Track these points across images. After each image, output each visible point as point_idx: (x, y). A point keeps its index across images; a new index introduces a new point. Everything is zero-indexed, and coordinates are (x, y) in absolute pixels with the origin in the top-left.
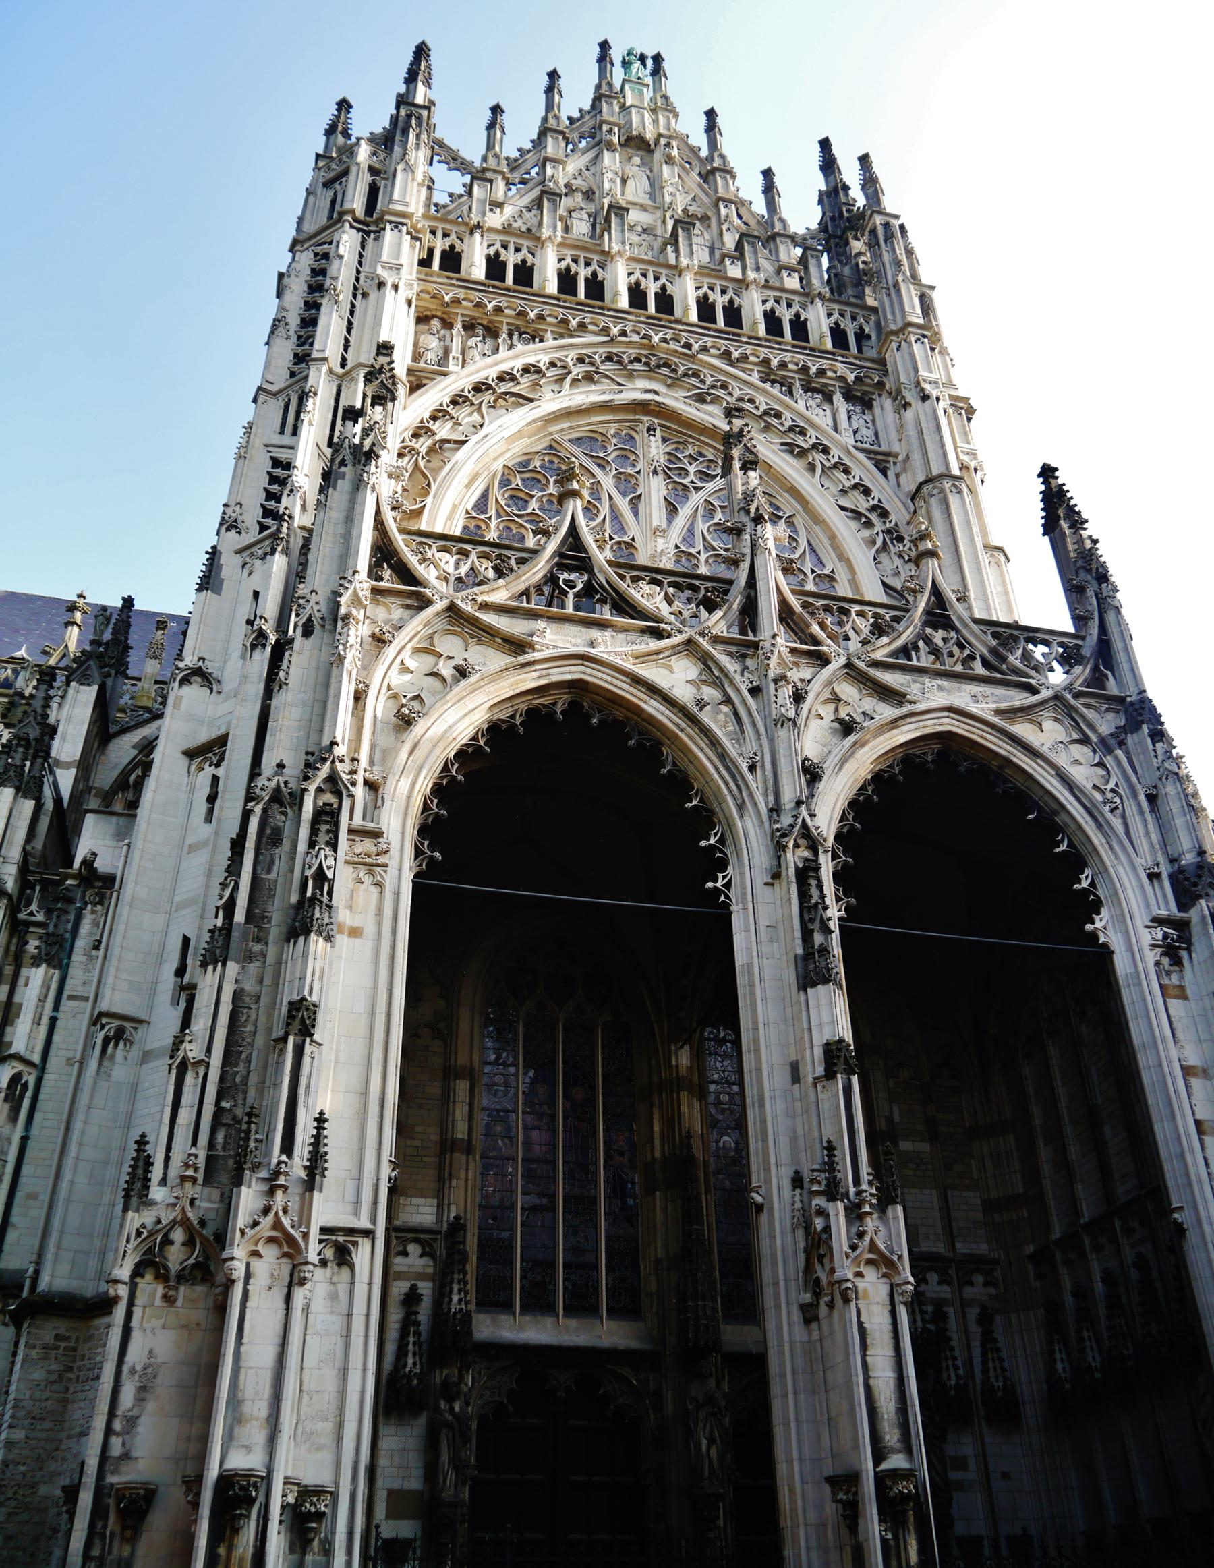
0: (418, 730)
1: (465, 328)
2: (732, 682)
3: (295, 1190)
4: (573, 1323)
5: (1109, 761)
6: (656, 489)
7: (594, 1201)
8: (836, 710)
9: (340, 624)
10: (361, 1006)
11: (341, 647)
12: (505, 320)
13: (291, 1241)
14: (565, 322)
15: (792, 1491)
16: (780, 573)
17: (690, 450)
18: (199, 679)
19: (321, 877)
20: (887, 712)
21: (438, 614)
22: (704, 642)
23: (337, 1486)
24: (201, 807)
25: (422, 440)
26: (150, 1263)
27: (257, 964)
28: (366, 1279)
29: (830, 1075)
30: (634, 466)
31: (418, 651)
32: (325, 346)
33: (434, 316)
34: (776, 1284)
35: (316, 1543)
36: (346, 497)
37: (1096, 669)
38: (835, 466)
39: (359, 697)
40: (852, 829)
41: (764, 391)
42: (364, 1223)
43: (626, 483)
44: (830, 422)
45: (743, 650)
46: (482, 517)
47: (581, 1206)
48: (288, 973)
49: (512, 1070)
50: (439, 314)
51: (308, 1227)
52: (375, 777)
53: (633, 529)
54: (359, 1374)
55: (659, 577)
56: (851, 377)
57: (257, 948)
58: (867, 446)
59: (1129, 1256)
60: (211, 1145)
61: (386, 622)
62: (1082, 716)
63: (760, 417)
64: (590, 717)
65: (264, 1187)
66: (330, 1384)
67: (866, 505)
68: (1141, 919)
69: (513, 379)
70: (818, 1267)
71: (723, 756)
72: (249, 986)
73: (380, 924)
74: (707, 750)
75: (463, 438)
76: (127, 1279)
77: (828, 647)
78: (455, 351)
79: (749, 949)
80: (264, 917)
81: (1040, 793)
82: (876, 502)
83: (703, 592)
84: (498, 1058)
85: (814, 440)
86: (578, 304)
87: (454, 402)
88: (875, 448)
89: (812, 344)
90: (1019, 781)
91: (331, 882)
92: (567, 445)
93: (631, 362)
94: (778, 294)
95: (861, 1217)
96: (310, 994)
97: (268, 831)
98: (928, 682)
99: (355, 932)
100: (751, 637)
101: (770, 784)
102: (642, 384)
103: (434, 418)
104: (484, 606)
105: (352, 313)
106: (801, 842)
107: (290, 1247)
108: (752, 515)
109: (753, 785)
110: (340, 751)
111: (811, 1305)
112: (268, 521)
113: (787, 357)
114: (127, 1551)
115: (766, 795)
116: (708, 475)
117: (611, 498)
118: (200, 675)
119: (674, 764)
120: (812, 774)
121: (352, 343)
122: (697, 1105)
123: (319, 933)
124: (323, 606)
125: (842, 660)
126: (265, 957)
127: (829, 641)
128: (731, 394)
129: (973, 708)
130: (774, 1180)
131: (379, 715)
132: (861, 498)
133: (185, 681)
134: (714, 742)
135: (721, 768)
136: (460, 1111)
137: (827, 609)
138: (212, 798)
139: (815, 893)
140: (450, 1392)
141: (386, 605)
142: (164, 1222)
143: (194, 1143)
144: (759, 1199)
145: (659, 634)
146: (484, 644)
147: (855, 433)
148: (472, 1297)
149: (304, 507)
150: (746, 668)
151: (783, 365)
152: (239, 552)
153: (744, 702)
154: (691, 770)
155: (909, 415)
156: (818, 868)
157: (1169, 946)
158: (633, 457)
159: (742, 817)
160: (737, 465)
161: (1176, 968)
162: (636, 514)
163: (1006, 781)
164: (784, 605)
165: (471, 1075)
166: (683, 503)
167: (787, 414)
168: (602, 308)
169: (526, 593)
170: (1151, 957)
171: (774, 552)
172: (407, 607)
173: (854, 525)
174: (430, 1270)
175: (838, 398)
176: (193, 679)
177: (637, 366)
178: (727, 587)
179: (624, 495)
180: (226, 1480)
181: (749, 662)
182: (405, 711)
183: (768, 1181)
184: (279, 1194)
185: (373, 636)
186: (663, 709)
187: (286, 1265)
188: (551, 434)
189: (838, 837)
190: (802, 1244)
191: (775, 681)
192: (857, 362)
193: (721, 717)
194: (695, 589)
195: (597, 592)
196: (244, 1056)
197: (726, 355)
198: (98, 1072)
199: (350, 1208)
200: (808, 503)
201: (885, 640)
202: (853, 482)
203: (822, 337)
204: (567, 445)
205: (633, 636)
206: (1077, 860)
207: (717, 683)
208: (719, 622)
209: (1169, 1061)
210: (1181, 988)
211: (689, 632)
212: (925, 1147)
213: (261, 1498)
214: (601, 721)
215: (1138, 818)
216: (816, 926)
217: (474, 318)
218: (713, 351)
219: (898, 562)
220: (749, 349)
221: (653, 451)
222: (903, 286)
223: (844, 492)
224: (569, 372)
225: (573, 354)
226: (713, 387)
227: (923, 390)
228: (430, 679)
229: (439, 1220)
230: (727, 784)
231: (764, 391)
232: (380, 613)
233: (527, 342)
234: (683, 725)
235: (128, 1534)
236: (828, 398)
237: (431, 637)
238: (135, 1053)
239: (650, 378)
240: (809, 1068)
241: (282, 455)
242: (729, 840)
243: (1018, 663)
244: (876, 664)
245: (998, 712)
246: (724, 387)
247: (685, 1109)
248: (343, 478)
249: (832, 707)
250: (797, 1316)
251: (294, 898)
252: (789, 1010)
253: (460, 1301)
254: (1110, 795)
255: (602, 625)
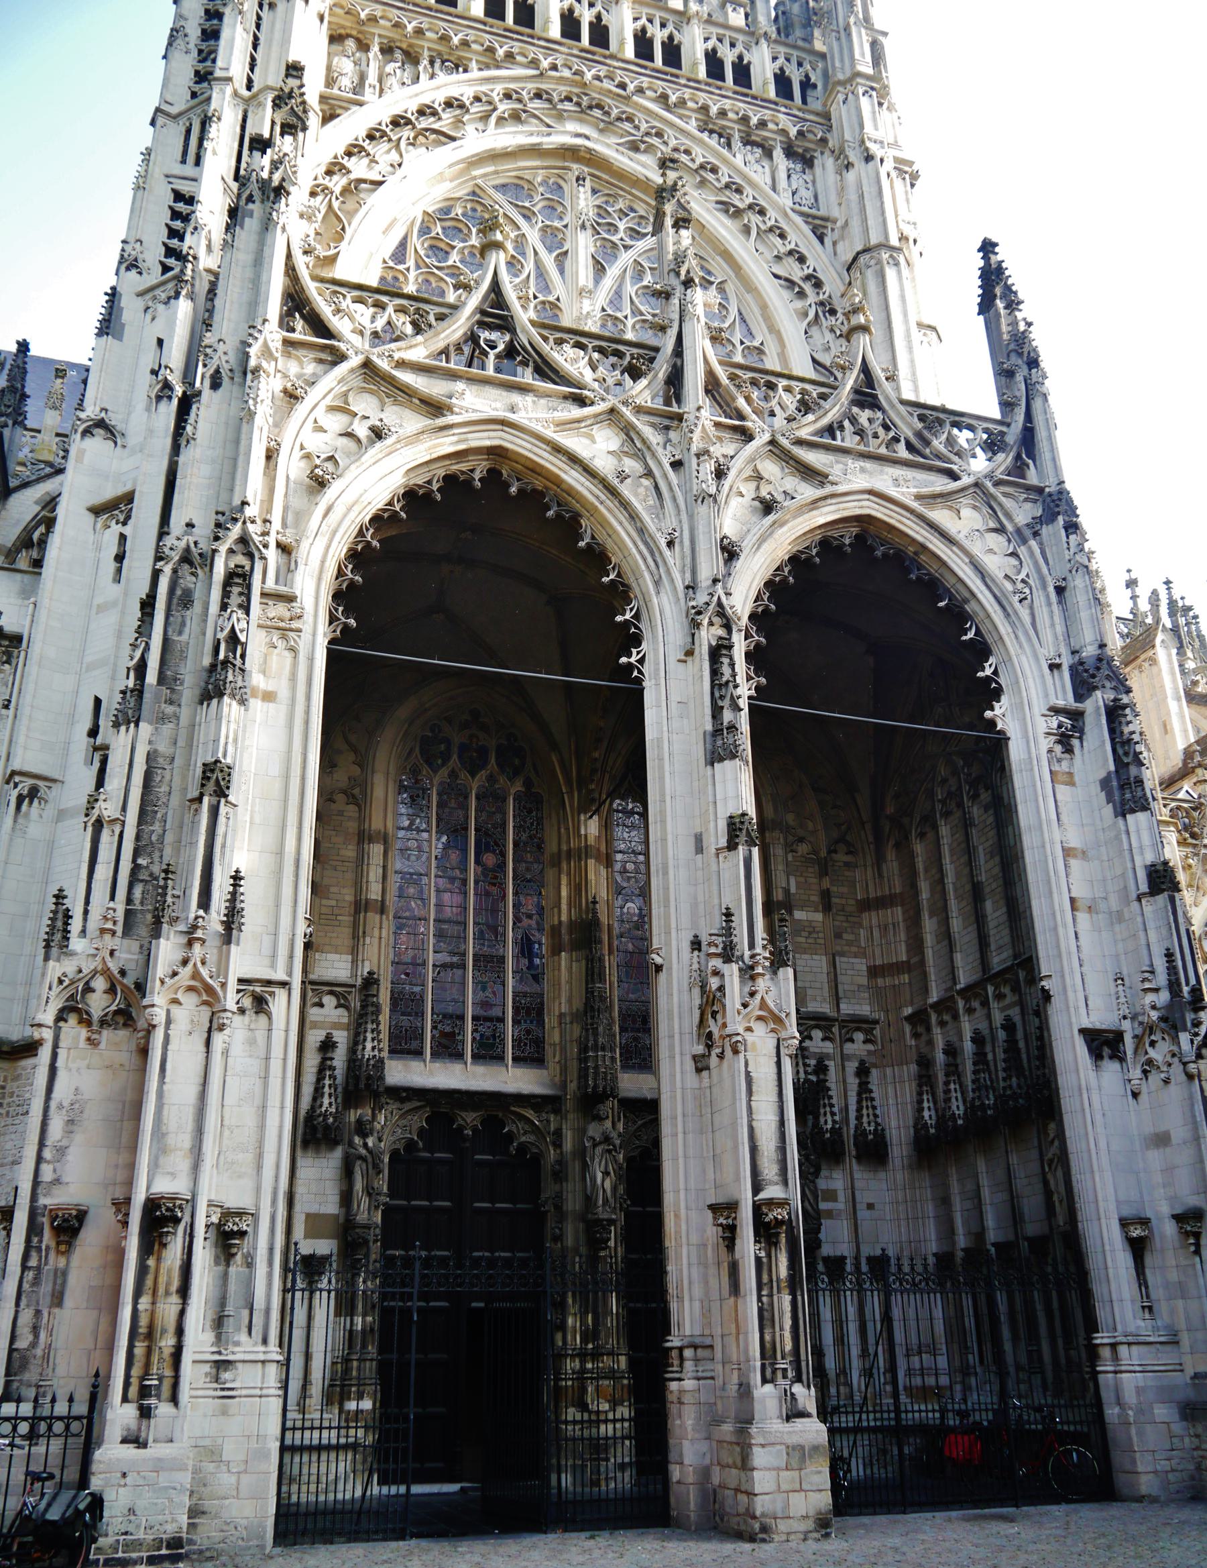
0: (331, 493)
1: (382, 51)
2: (654, 455)
3: (213, 943)
4: (480, 1069)
5: (1022, 551)
6: (584, 246)
7: (502, 960)
8: (758, 488)
9: (249, 376)
10: (275, 769)
11: (251, 402)
12: (426, 44)
13: (209, 990)
14: (491, 50)
15: (677, 1216)
16: (707, 343)
17: (621, 204)
18: (101, 432)
19: (233, 639)
20: (808, 492)
21: (352, 371)
22: (627, 412)
23: (258, 1208)
24: (112, 566)
25: (336, 178)
26: (72, 1009)
27: (171, 725)
28: (283, 1026)
29: (732, 846)
30: (561, 218)
31: (332, 409)
32: (229, 63)
33: (349, 36)
34: (671, 1037)
35: (239, 1257)
36: (254, 238)
37: (1018, 457)
38: (771, 230)
39: (270, 455)
40: (766, 610)
41: (701, 142)
42: (280, 975)
43: (552, 238)
44: (769, 181)
45: (666, 422)
46: (401, 267)
47: (490, 964)
48: (202, 735)
49: (425, 835)
50: (354, 33)
51: (226, 977)
52: (287, 540)
53: (559, 289)
54: (277, 1111)
55: (584, 340)
56: (793, 132)
57: (169, 709)
58: (806, 209)
59: (998, 1018)
60: (129, 901)
61: (299, 376)
62: (1000, 505)
63: (696, 171)
64: (508, 486)
65: (183, 940)
66: (249, 1119)
67: (801, 274)
68: (1039, 707)
69: (434, 113)
70: (711, 1022)
71: (642, 531)
72: (163, 747)
73: (293, 689)
74: (626, 524)
75: (380, 178)
76: (51, 1023)
77: (753, 423)
78: (372, 78)
79: (659, 723)
80: (176, 680)
81: (953, 580)
82: (810, 271)
83: (628, 358)
84: (412, 824)
85: (751, 200)
86: (506, 30)
87: (371, 137)
88: (813, 211)
89: (754, 91)
90: (933, 568)
91: (244, 646)
92: (491, 191)
93: (562, 101)
94: (721, 31)
95: (753, 978)
96: (225, 756)
97: (179, 592)
98: (853, 464)
99: (269, 697)
100: (675, 408)
101: (688, 560)
102: (571, 126)
103: (349, 154)
104: (402, 364)
105: (258, 26)
106: (716, 620)
107: (209, 995)
108: (683, 277)
109: (671, 561)
110: (249, 512)
111: (703, 1056)
112: (171, 262)
113: (727, 104)
114: (62, 1262)
115: (683, 572)
116: (638, 233)
117: (536, 253)
118: (102, 426)
119: (593, 537)
120: (730, 553)
121: (259, 61)
122: (603, 872)
123: (233, 696)
124: (232, 357)
125: (767, 437)
126: (178, 718)
127: (754, 417)
128: (665, 143)
129: (893, 492)
130: (674, 943)
131: (292, 477)
132: (796, 266)
133: (87, 432)
134: (633, 516)
135: (640, 543)
136: (374, 874)
137: (754, 383)
138: (120, 558)
139: (726, 670)
140: (362, 1129)
141: (298, 359)
142: (85, 971)
143: (112, 898)
144: (658, 960)
145: (581, 401)
146: (401, 404)
147: (794, 194)
148: (385, 1045)
149: (209, 248)
150: (669, 440)
151: (723, 113)
152: (140, 294)
153: (665, 476)
154: (609, 545)
155: (851, 176)
156: (730, 647)
157: (1063, 735)
158: (560, 209)
159: (658, 593)
160: (669, 222)
161: (1067, 756)
162: (562, 271)
163: (920, 567)
164: (711, 375)
165: (385, 839)
166: (611, 263)
167: (724, 170)
168: (532, 37)
169: (445, 352)
170: (1045, 743)
171: (703, 320)
172: (321, 361)
173: (786, 294)
174: (345, 1020)
175: (778, 154)
176: (96, 431)
177: (568, 106)
178: (653, 354)
179: (550, 251)
180: (152, 1204)
181: (672, 435)
182: (318, 471)
183: (668, 943)
184: (197, 947)
185: (285, 391)
186: (583, 479)
187: (206, 1013)
188: (475, 178)
189: (753, 617)
190: (697, 1002)
191: (698, 456)
192: (800, 114)
193: (641, 490)
194: (619, 354)
195: (519, 354)
196: (159, 815)
197: (663, 98)
198: (13, 829)
199: (267, 961)
200: (740, 268)
201: (810, 417)
202: (789, 247)
203: (765, 84)
204: (491, 191)
205: (555, 402)
206: (981, 650)
207: (639, 455)
208: (644, 391)
209: (1052, 843)
210: (1070, 774)
211: (611, 401)
212: (819, 917)
213: (186, 1219)
214: (520, 491)
215: (1045, 609)
216: (726, 703)
217: (392, 40)
218: (649, 93)
219: (829, 336)
220: (687, 94)
221: (582, 203)
222: (854, 30)
223: (778, 258)
224: (495, 109)
225: (499, 88)
226: (648, 134)
227: (867, 149)
228: (345, 440)
229: (354, 975)
230: (645, 560)
231: (701, 142)
232: (293, 368)
233: (449, 71)
234: (603, 497)
235: (63, 1248)
236: (768, 153)
237: (345, 395)
238: (50, 811)
239: (581, 121)
240: (713, 839)
241: (185, 187)
242: (644, 616)
243: (942, 448)
244: (800, 442)
245: (919, 497)
246: (659, 134)
247: (591, 876)
248: (251, 216)
249: (753, 485)
250: (690, 1065)
251: (207, 661)
252: (696, 784)
253: (373, 1048)
254: (1020, 586)
255: (523, 389)
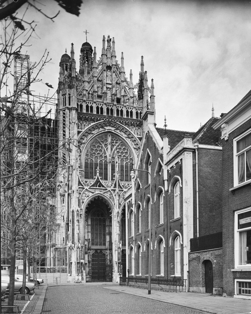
6: (109, 147)
179: (106, 147)
